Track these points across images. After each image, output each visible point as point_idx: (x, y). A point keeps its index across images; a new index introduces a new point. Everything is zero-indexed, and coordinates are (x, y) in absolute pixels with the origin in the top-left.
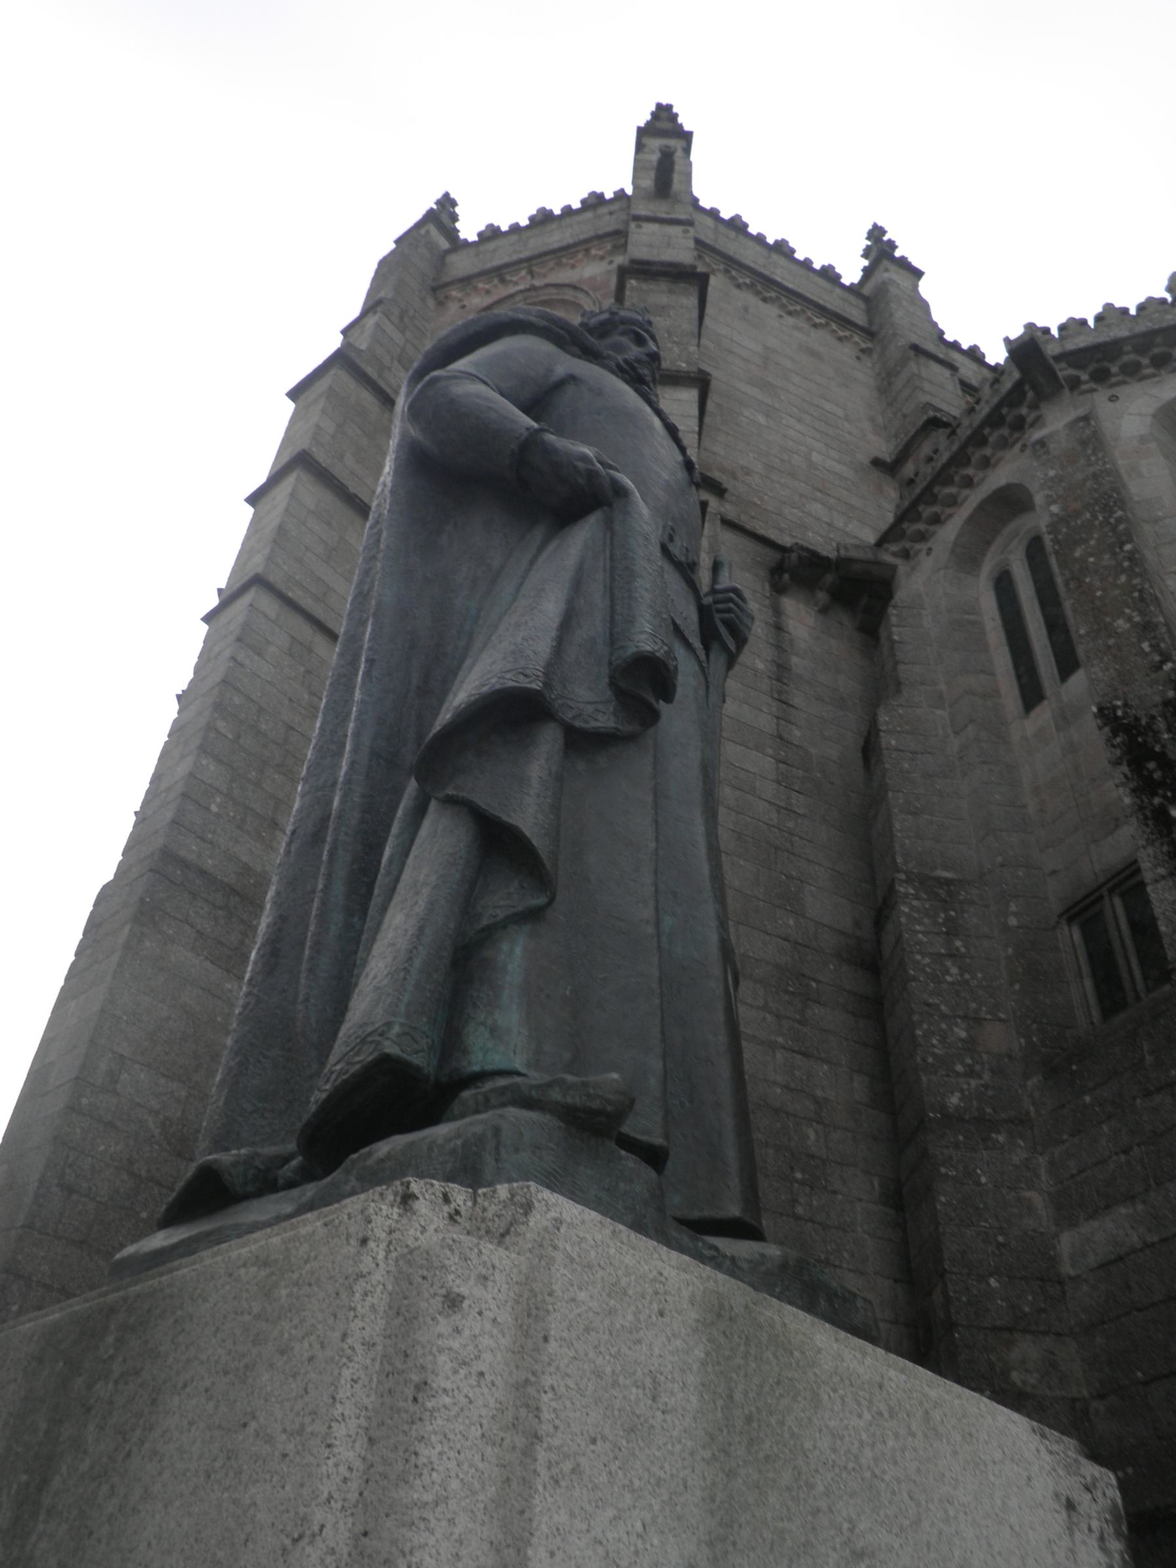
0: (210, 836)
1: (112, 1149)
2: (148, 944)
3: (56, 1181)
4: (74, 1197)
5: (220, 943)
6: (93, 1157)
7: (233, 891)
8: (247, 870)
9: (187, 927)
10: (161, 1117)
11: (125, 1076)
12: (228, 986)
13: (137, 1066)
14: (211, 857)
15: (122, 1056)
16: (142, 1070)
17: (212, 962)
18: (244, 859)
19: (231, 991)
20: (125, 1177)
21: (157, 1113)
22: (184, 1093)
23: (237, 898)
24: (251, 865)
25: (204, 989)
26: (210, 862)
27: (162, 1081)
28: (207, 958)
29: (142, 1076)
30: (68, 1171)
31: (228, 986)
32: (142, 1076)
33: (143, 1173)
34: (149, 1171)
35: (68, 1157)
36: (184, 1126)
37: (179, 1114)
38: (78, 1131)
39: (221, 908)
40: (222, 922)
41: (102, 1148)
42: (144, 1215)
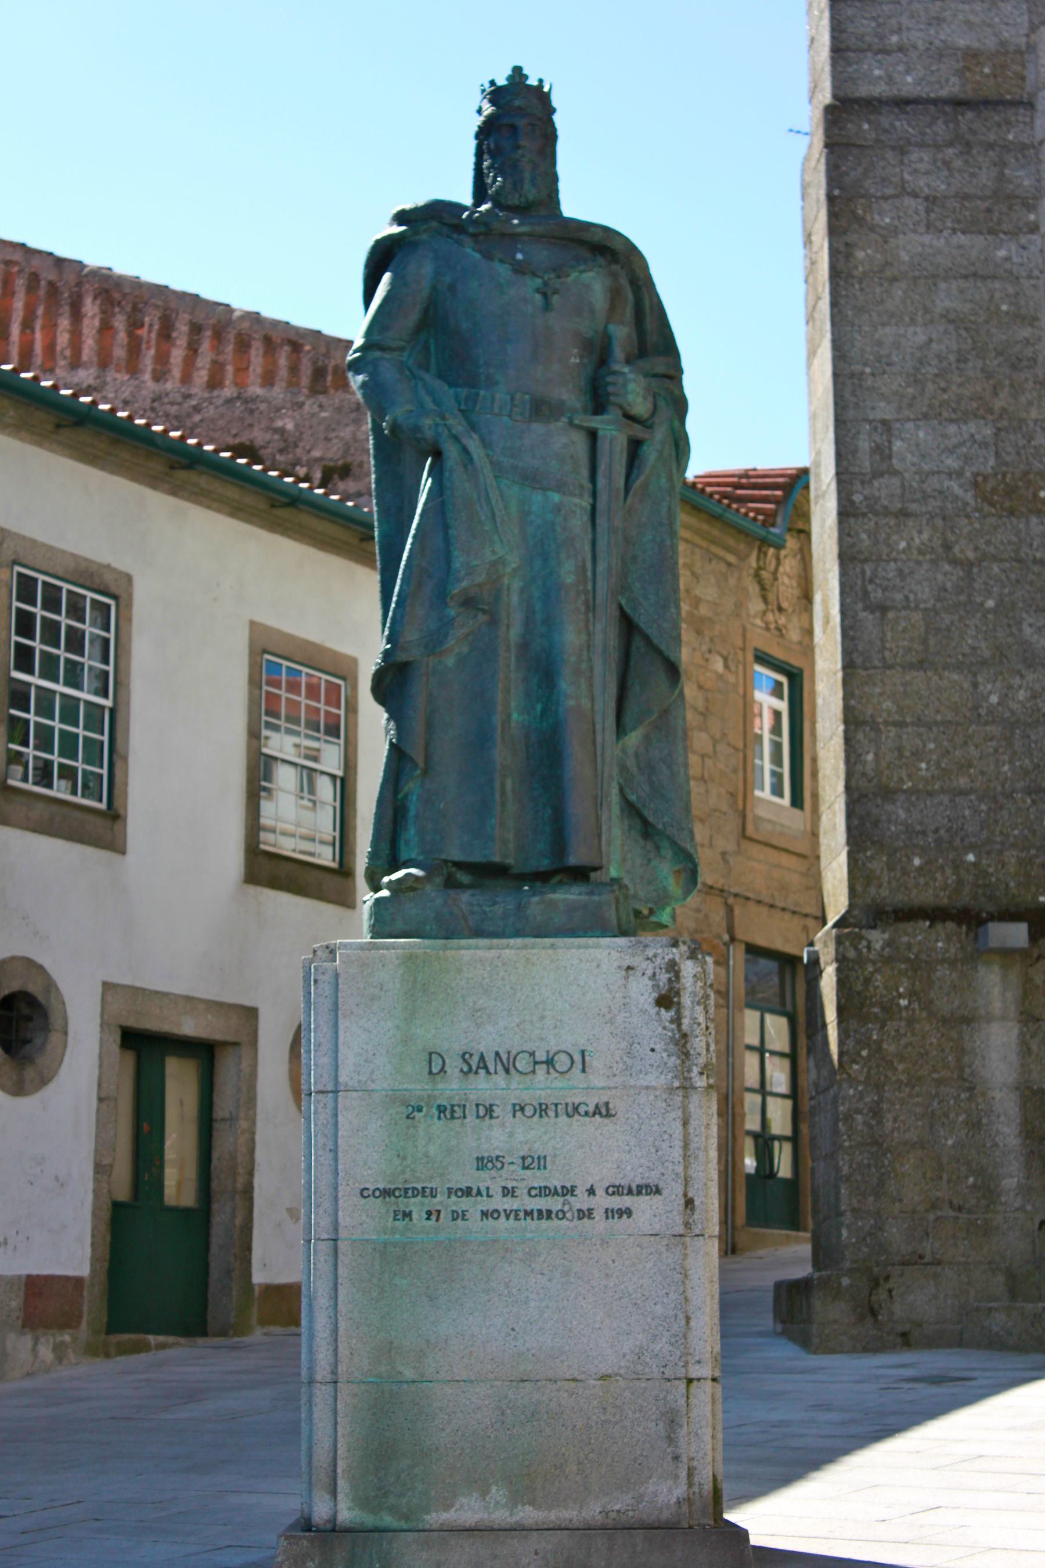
0: (894, 39)
1: (917, 541)
2: (860, 255)
3: (860, 605)
4: (891, 615)
5: (965, 197)
6: (895, 560)
7: (959, 104)
8: (972, 56)
9: (908, 201)
10: (968, 474)
11: (898, 445)
12: (1002, 253)
13: (910, 425)
14: (908, 72)
15: (884, 422)
16: (918, 427)
17: (964, 232)
18: (962, 43)
19: (1008, 259)
20: (947, 567)
21: (960, 474)
22: (988, 431)
23: (970, 115)
24: (976, 45)
25: (966, 277)
26: (909, 79)
27: (952, 429)
28: (954, 231)
29: (921, 434)
30: (870, 588)
31: (1002, 253)
32: (921, 434)
33: (971, 555)
34: (976, 548)
35: (863, 572)
36: (1004, 475)
37: (992, 462)
38: (864, 536)
39: (950, 144)
40: (958, 163)
41: (903, 545)
42: (990, 603)
